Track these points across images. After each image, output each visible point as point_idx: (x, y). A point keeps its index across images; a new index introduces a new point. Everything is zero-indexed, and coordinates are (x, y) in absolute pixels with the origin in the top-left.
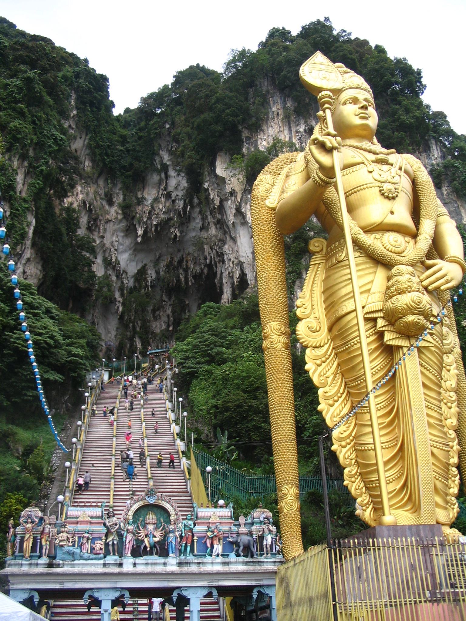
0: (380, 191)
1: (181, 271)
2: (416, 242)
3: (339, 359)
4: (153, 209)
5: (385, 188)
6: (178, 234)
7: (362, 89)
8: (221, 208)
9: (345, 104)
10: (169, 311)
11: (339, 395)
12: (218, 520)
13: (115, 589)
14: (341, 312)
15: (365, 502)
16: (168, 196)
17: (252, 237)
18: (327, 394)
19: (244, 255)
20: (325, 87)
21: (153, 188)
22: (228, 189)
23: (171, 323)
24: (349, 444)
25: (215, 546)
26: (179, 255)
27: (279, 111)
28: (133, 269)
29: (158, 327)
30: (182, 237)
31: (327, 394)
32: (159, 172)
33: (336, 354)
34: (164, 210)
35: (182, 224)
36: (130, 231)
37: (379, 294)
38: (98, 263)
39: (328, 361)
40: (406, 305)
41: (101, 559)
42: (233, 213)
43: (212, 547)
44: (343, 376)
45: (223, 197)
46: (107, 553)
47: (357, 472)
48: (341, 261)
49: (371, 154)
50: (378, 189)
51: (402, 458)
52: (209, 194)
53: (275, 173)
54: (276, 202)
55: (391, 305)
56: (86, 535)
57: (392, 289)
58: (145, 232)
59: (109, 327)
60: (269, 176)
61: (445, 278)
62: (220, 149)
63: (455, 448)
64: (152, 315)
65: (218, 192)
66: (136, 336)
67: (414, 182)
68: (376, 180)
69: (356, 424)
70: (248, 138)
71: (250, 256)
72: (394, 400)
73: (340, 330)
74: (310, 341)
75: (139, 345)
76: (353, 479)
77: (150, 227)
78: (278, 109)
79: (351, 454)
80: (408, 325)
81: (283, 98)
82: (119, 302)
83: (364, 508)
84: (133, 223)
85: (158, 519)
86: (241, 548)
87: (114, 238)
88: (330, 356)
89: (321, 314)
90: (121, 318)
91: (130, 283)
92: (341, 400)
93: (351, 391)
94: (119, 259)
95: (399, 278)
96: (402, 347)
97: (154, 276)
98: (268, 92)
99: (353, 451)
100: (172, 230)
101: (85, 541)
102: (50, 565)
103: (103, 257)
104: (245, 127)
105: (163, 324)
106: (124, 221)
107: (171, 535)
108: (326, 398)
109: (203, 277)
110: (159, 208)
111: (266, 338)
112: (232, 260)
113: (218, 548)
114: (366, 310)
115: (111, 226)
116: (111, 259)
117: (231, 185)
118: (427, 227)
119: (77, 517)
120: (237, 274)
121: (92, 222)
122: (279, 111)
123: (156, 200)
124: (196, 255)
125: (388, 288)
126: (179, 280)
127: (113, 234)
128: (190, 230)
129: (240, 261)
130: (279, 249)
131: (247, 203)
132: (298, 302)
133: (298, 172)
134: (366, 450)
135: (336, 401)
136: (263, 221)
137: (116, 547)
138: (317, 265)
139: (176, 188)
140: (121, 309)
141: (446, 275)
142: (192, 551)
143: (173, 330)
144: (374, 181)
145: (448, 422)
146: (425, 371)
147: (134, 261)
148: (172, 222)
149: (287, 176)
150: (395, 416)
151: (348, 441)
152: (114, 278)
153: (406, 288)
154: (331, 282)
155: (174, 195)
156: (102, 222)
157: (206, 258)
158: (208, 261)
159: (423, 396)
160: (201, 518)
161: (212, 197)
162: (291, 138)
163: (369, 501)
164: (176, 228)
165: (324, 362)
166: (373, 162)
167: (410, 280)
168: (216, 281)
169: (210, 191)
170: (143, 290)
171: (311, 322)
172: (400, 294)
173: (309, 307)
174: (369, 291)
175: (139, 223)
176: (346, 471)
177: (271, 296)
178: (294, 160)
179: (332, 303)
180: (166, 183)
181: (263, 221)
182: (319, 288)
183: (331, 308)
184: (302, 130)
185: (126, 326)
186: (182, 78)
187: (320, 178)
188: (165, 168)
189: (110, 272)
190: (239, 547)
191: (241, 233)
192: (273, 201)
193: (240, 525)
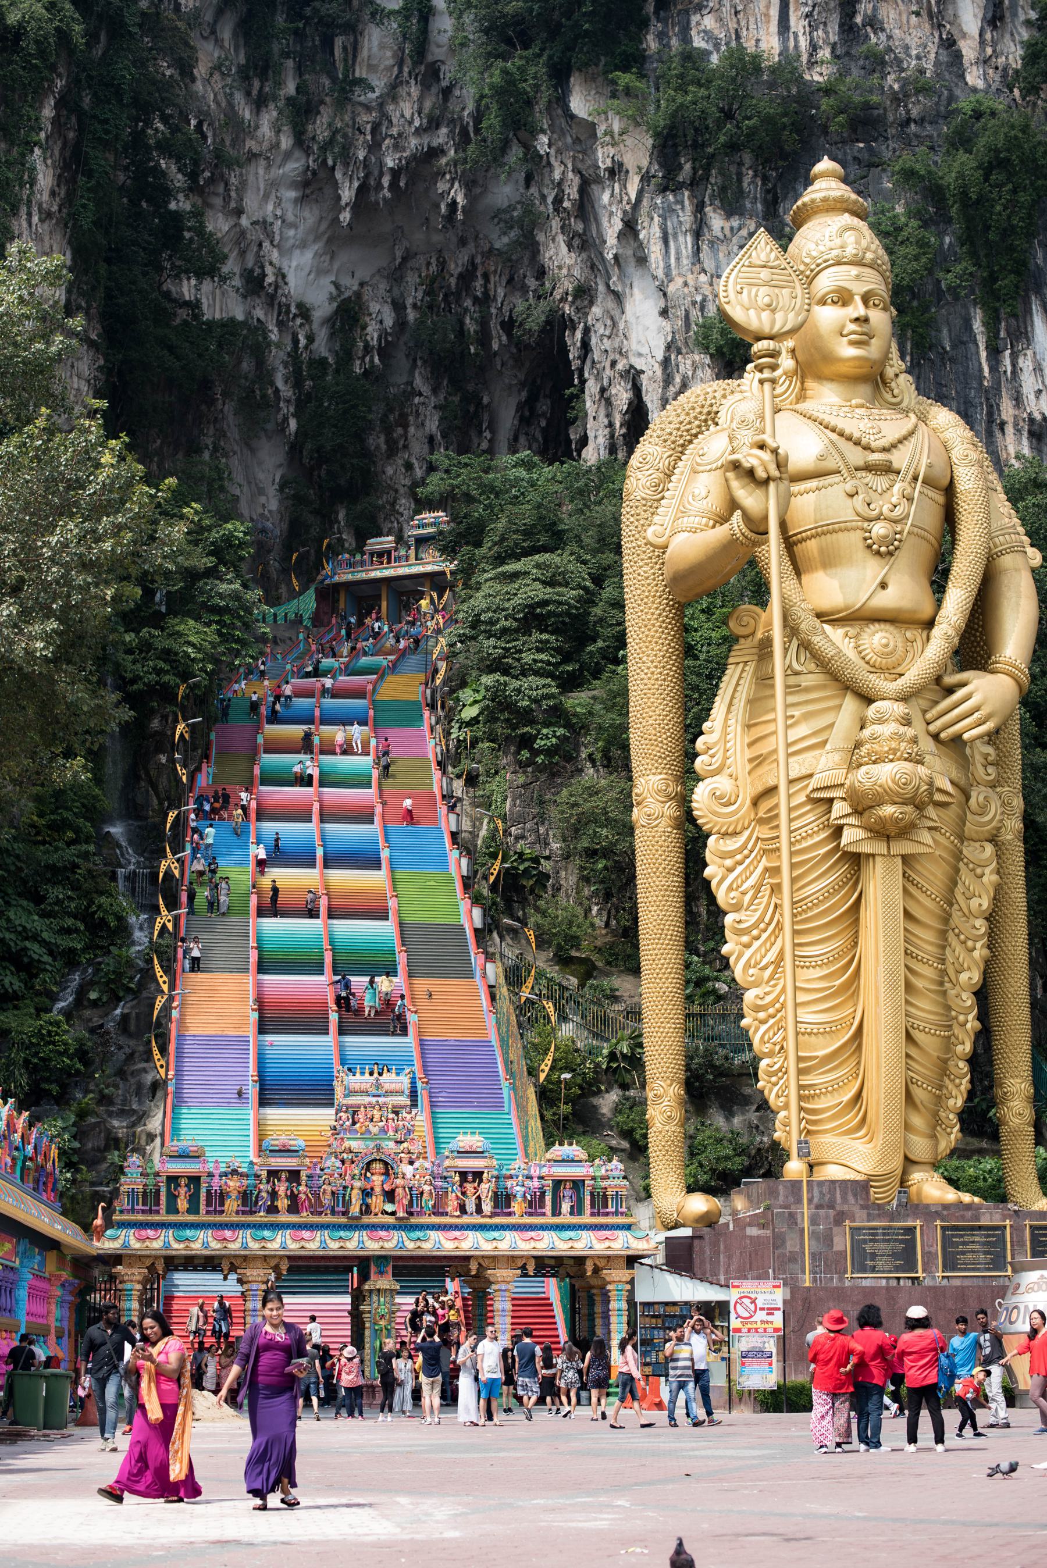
1: (468, 303)
6: (460, 199)
16: (433, 73)
19: (645, 350)
26: (463, 257)
34: (417, 123)
36: (314, 185)
39: (748, 861)
50: (859, 534)
51: (859, 1047)
57: (864, 750)
59: (261, 476)
61: (976, 715)
63: (969, 1026)
65: (574, 158)
67: (950, 491)
72: (856, 943)
77: (376, 173)
80: (882, 820)
82: (288, 401)
84: (325, 161)
87: (270, 207)
90: (295, 449)
96: (873, 855)
100: (442, 186)
106: (297, 154)
110: (403, 116)
114: (813, 783)
115: (261, 171)
116: (264, 275)
121: (207, 174)
126: (461, 332)
127: (266, 197)
129: (632, 367)
131: (652, 219)
132: (700, 743)
133: (714, 466)
135: (757, 938)
136: (643, 556)
140: (293, 424)
171: (722, 783)
172: (874, 762)
173: (719, 756)
178: (715, 409)
181: (643, 556)
191: (635, 284)
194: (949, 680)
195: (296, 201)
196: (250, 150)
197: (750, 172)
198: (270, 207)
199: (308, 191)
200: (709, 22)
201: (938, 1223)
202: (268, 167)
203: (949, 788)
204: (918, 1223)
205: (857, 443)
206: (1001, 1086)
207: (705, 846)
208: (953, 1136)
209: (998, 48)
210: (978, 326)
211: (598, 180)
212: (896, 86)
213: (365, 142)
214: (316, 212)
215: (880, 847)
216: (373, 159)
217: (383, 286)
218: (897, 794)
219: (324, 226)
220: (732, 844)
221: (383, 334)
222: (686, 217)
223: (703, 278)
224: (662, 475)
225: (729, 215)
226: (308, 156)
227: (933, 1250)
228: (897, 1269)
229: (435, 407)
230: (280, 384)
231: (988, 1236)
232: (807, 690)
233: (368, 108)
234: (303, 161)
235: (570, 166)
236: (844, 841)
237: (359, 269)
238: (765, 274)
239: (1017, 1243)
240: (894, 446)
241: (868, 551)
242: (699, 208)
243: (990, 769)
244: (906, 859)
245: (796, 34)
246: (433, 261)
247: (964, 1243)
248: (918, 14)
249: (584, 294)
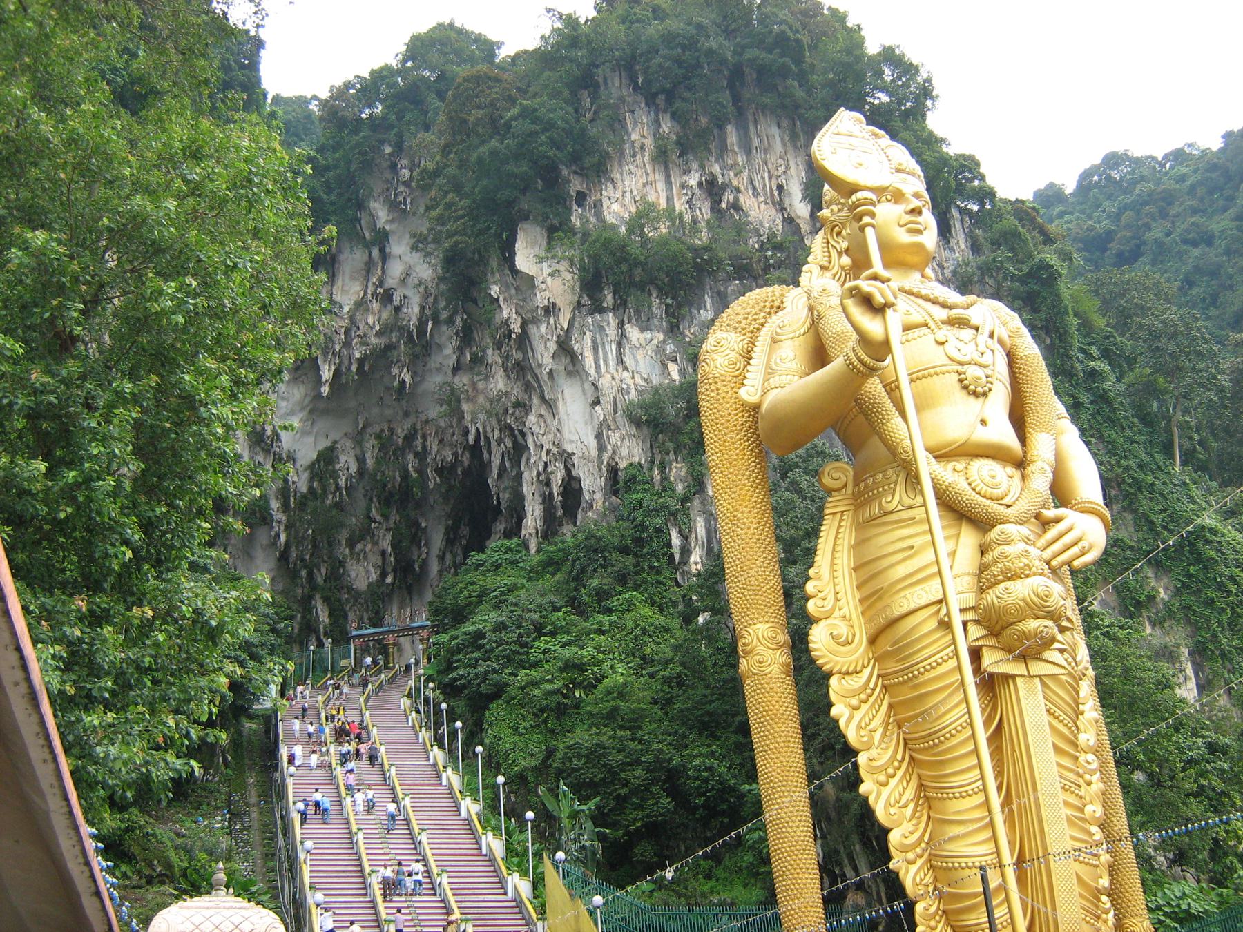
0: (961, 381)
1: (410, 457)
2: (1023, 477)
3: (891, 697)
5: (969, 375)
6: (408, 380)
8: (524, 340)
10: (386, 544)
11: (896, 764)
14: (897, 611)
16: (387, 297)
17: (596, 402)
18: (874, 764)
19: (575, 438)
20: (862, 182)
21: (352, 278)
22: (541, 300)
23: (389, 569)
26: (408, 424)
27: (645, 141)
28: (307, 452)
29: (362, 574)
30: (414, 385)
31: (874, 764)
32: (368, 246)
33: (884, 687)
34: (377, 328)
35: (415, 358)
39: (872, 699)
40: (1024, 600)
42: (552, 351)
44: (900, 727)
45: (528, 316)
47: (938, 909)
48: (892, 512)
49: (937, 308)
50: (955, 377)
54: (760, 393)
55: (995, 601)
58: (337, 373)
60: (733, 335)
61: (1080, 544)
62: (526, 217)
63: (1103, 859)
66: (318, 596)
69: (929, 817)
70: (581, 198)
71: (592, 443)
73: (895, 643)
74: (837, 663)
75: (324, 616)
76: (933, 923)
77: (346, 362)
78: (643, 136)
80: (1025, 635)
81: (652, 114)
82: (279, 522)
88: (874, 690)
89: (853, 611)
90: (284, 557)
91: (301, 482)
92: (900, 773)
93: (914, 755)
95: (1010, 550)
96: (1013, 677)
97: (354, 468)
98: (622, 100)
100: (395, 371)
104: (575, 172)
105: (372, 570)
108: (873, 771)
109: (459, 471)
111: (746, 653)
112: (547, 446)
117: (547, 294)
118: (1042, 446)
120: (558, 477)
122: (645, 141)
123: (361, 305)
124: (442, 424)
126: (405, 476)
128: (430, 370)
129: (565, 451)
134: (956, 869)
135: (893, 776)
138: (839, 515)
139: (403, 281)
140: (283, 538)
143: (393, 584)
144: (947, 361)
146: (1055, 723)
147: (309, 433)
148: (396, 353)
149: (774, 341)
151: (918, 850)
154: (871, 551)
155: (397, 296)
157: (466, 433)
158: (471, 440)
159: (1055, 769)
162: (670, 199)
164: (403, 366)
165: (865, 702)
166: (943, 323)
167: (1026, 554)
168: (489, 481)
170: (330, 497)
172: (1009, 579)
173: (831, 597)
176: (919, 908)
177: (753, 572)
178: (777, 304)
179: (877, 591)
180: (383, 271)
182: (845, 561)
183: (876, 601)
184: (693, 182)
185: (293, 575)
186: (419, 48)
187: (861, 361)
188: (382, 239)
192: (753, 389)
194: (1050, 513)
205: (935, 302)
207: (828, 687)
217: (349, 444)
219: (308, 399)
220: (856, 682)
222: (612, 331)
223: (625, 374)
225: (642, 330)
237: (332, 432)
241: (964, 392)
242: (621, 325)
248: (766, 203)
249: (522, 407)
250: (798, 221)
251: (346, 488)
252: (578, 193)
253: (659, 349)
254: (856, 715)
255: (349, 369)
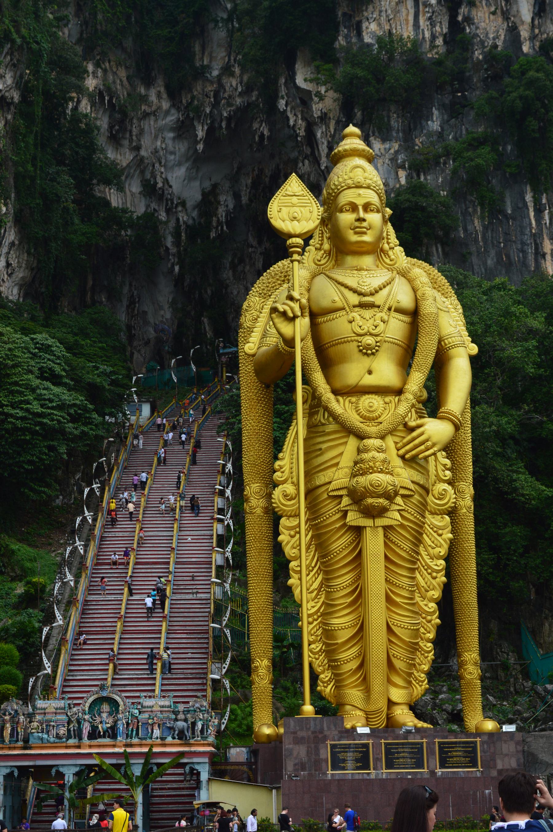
0: (359, 346)
2: (399, 401)
4: (221, 86)
6: (266, 133)
7: (365, 188)
9: (341, 211)
11: (311, 568)
12: (159, 709)
13: (76, 765)
15: (327, 679)
20: (292, 232)
24: (317, 620)
25: (155, 731)
28: (193, 194)
34: (240, 89)
36: (183, 130)
37: (346, 470)
38: (133, 194)
40: (365, 488)
41: (63, 742)
43: (152, 732)
46: (69, 737)
47: (321, 649)
52: (288, 119)
53: (265, 294)
56: (52, 724)
58: (210, 132)
63: (433, 622)
64: (231, 273)
65: (302, 112)
68: (355, 333)
74: (285, 511)
76: (317, 656)
77: (219, 120)
79: (317, 630)
83: (325, 685)
84: (188, 115)
85: (111, 708)
86: (177, 732)
90: (178, 282)
94: (170, 178)
96: (365, 527)
99: (320, 627)
100: (255, 125)
101: (51, 728)
102: (25, 748)
103: (141, 181)
106: (173, 111)
107: (119, 722)
110: (231, 86)
113: (157, 732)
114: (331, 487)
115: (152, 123)
119: (45, 709)
121: (117, 127)
125: (356, 463)
127: (156, 137)
130: (265, 394)
132: (277, 464)
137: (76, 732)
140: (177, 268)
141: (427, 440)
142: (137, 734)
145: (431, 593)
150: (359, 596)
151: (315, 617)
152: (163, 216)
153: (367, 468)
156: (135, 121)
160: (145, 707)
161: (292, 123)
163: (331, 678)
166: (354, 306)
169: (289, 114)
173: (287, 472)
174: (337, 464)
175: (199, 117)
189: (154, 205)
190: (175, 731)
193: (179, 712)
194: (412, 424)
195: (174, 139)
196: (145, 111)
197: (395, 115)
198: (159, 143)
199: (181, 133)
200: (373, 26)
201: (383, 741)
202: (156, 121)
203: (412, 486)
204: (371, 742)
205: (355, 291)
206: (460, 656)
208: (423, 687)
209: (542, 30)
210: (529, 197)
211: (316, 124)
212: (481, 57)
213: (210, 102)
214: (186, 144)
215: (368, 522)
216: (216, 112)
218: (375, 492)
219: (191, 152)
221: (228, 213)
224: (258, 313)
225: (384, 140)
226: (179, 112)
227: (379, 757)
228: (358, 768)
229: (261, 254)
230: (169, 245)
231: (412, 748)
232: (329, 434)
233: (212, 83)
234: (176, 116)
235: (300, 116)
236: (348, 520)
238: (295, 200)
239: (431, 752)
240: (377, 292)
243: (448, 473)
244: (387, 529)
245: (423, 30)
246: (256, 168)
247: (398, 753)
248: (494, 13)
250: (521, 28)
251: (227, 223)
252: (344, 14)
253: (393, 160)
254: (295, 539)
255: (221, 127)
